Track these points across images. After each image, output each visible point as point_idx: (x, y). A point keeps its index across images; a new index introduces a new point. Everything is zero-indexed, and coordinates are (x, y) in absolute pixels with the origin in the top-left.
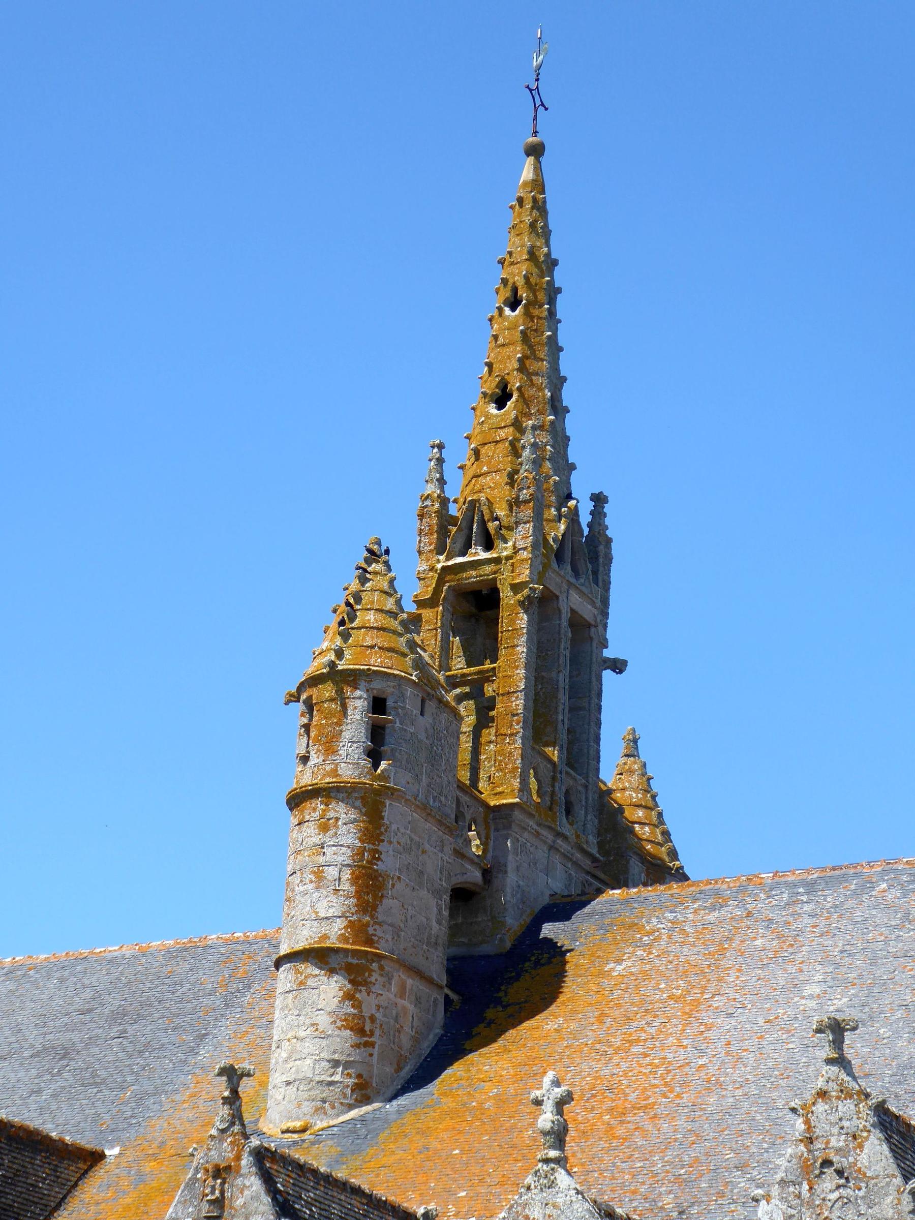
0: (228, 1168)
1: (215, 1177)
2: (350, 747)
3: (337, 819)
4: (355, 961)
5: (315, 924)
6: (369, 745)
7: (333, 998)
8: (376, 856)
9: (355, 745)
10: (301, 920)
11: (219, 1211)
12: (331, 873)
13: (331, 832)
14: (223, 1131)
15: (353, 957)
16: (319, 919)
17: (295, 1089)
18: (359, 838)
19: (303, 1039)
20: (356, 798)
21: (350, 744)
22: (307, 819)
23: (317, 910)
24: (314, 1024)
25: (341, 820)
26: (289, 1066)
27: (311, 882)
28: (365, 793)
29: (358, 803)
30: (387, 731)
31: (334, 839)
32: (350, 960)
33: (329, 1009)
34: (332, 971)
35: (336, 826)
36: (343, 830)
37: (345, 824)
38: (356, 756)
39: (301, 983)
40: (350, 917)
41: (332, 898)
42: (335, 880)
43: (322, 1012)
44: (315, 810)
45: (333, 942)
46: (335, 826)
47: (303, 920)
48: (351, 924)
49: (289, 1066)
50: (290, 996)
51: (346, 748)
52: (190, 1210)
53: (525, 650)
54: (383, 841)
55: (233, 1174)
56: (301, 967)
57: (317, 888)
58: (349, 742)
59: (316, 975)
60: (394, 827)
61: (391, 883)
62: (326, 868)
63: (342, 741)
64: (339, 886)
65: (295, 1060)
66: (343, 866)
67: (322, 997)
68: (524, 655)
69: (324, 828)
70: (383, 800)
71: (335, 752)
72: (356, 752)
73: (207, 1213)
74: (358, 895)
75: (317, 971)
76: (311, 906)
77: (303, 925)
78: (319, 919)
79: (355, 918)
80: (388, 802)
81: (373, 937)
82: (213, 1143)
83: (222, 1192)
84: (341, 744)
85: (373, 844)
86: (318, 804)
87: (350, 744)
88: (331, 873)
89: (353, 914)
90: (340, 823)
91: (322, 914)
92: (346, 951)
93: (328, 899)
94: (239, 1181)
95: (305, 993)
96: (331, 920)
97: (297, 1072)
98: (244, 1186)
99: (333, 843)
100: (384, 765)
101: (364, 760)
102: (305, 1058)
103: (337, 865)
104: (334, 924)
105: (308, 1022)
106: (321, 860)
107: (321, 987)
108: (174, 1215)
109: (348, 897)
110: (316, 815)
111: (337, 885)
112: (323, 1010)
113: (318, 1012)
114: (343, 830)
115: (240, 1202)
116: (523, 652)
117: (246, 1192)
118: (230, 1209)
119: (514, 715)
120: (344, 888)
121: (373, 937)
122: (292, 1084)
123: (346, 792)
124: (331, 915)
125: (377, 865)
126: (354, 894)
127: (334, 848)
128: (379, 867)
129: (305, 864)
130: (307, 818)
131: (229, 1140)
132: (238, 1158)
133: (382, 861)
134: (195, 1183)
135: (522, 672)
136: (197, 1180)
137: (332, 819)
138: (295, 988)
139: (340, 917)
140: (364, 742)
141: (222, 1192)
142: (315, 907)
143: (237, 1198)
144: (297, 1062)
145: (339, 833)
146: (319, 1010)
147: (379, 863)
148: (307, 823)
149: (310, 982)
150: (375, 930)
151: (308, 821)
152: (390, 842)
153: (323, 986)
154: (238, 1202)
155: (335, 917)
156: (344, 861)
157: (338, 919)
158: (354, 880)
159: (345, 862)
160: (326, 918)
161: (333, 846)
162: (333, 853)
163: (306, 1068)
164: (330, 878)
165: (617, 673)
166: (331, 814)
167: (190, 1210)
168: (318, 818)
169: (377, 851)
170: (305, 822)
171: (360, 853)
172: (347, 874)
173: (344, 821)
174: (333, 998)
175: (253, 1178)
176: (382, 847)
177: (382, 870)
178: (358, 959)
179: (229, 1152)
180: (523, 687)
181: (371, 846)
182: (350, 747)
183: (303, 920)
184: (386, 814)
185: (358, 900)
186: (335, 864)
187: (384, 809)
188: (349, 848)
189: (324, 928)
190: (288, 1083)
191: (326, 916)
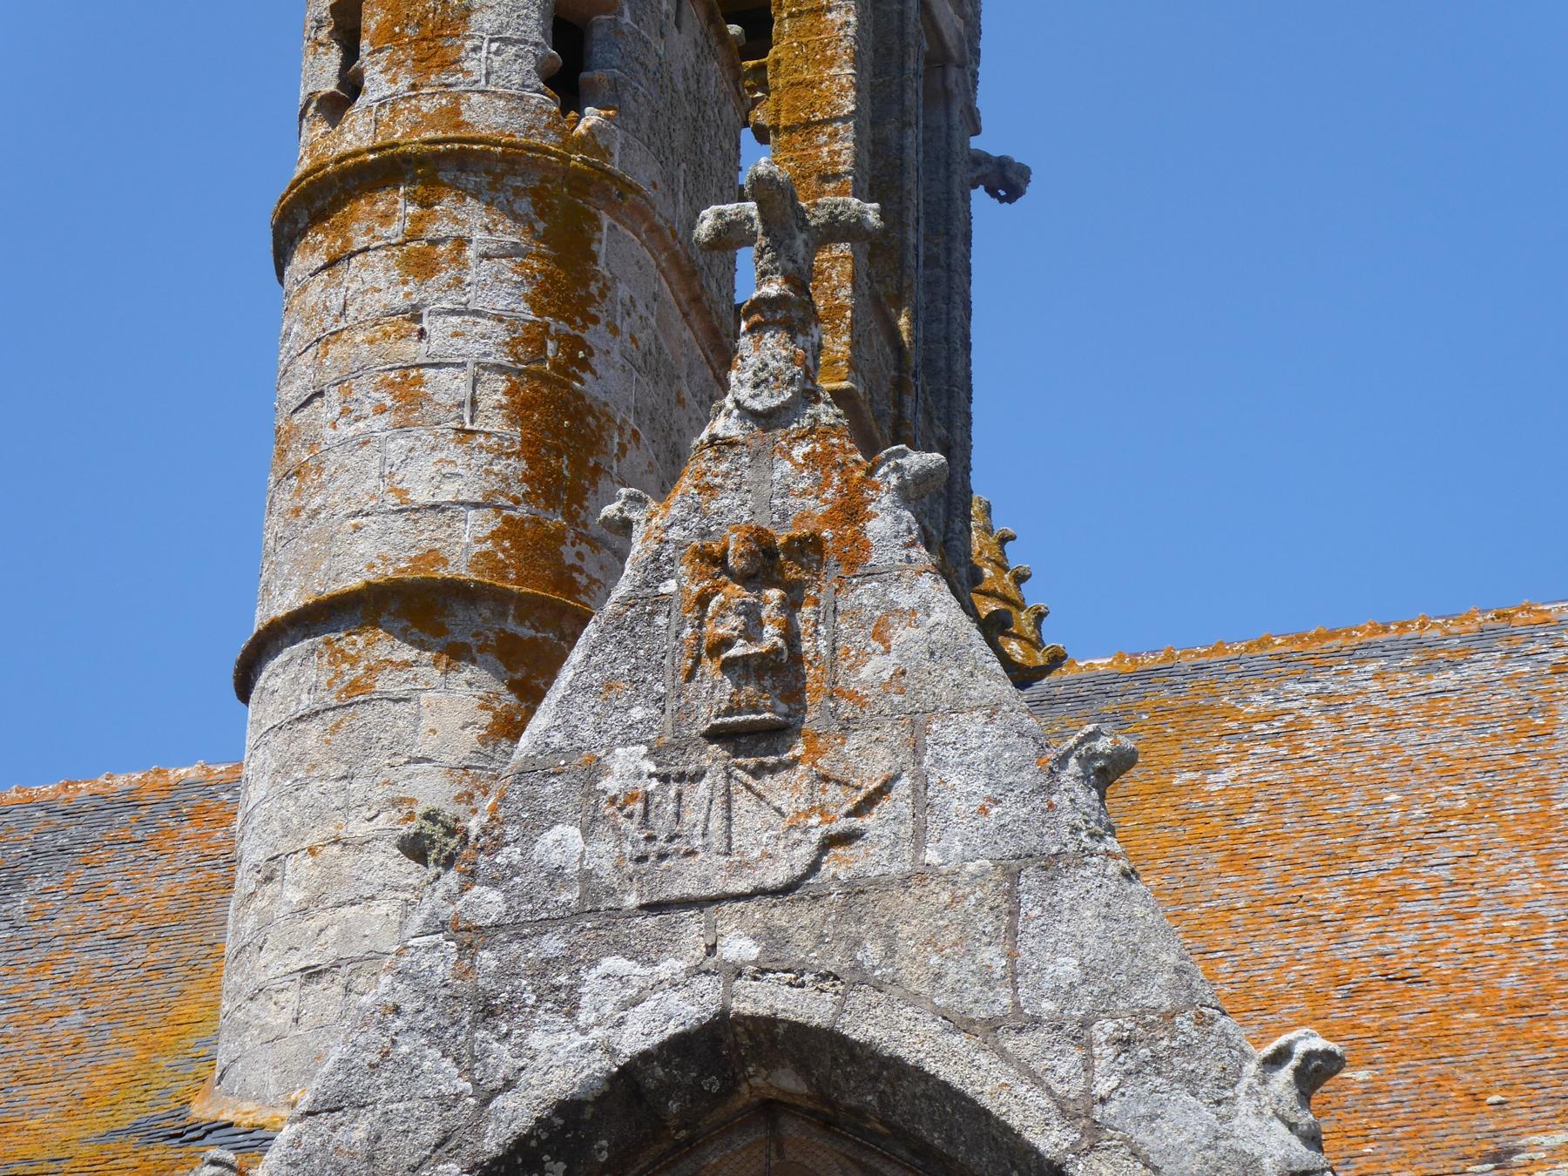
0: (808, 548)
1: (754, 578)
2: (497, 53)
3: (462, 243)
4: (526, 632)
5: (399, 522)
6: (552, 56)
7: (463, 728)
8: (577, 358)
9: (512, 50)
10: (348, 516)
11: (783, 708)
12: (448, 385)
13: (444, 277)
14: (766, 420)
15: (521, 619)
16: (408, 510)
17: (337, 989)
18: (528, 299)
19: (363, 844)
20: (517, 192)
21: (494, 46)
22: (361, 247)
23: (404, 485)
24: (403, 801)
25: (473, 245)
26: (314, 925)
27: (381, 410)
28: (542, 181)
29: (524, 205)
30: (598, 33)
31: (453, 295)
32: (511, 625)
33: (449, 759)
34: (457, 654)
35: (457, 258)
36: (478, 272)
37: (486, 256)
38: (516, 79)
39: (354, 686)
40: (507, 508)
41: (453, 452)
42: (461, 405)
43: (425, 765)
44: (386, 218)
45: (459, 568)
46: (454, 260)
47: (355, 515)
48: (511, 529)
49: (314, 925)
50: (314, 729)
51: (484, 53)
52: (637, 713)
53: (852, 19)
54: (595, 320)
55: (833, 570)
56: (354, 643)
57: (401, 427)
58: (491, 41)
59: (407, 664)
60: (623, 291)
61: (616, 440)
62: (431, 372)
63: (472, 37)
64: (472, 422)
65: (339, 905)
66: (485, 368)
67: (427, 722)
68: (851, 31)
69: (421, 265)
70: (592, 210)
71: (450, 64)
72: (516, 67)
73: (729, 712)
74: (531, 450)
75: (407, 653)
76: (382, 476)
77: (357, 528)
78: (408, 510)
79: (521, 512)
80: (606, 220)
81: (575, 575)
82: (724, 467)
83: (791, 635)
84: (469, 44)
85: (570, 322)
86: (401, 206)
87: (494, 46)
88: (448, 385)
89: (517, 502)
90: (470, 253)
91: (421, 496)
92: (501, 598)
93: (439, 455)
94: (865, 595)
95: (370, 714)
96: (450, 513)
97: (345, 937)
98: (893, 610)
99: (450, 306)
100: (592, 117)
101: (538, 91)
102: (373, 898)
103: (464, 364)
104: (462, 525)
105: (379, 794)
106: (413, 350)
107: (423, 695)
108: (557, 739)
109: (500, 454)
110: (395, 230)
111: (467, 420)
112: (429, 760)
113: (412, 767)
114: (478, 272)
115: (875, 668)
116: (847, 24)
117: (901, 634)
118: (831, 697)
119: (825, 178)
120: (487, 429)
121: (575, 575)
122: (328, 977)
123: (488, 172)
124: (449, 498)
125: (582, 381)
126: (518, 447)
127: (455, 320)
128: (587, 385)
129: (358, 364)
130: (360, 241)
131: (799, 452)
132: (852, 511)
133: (594, 373)
134: (652, 614)
135: (845, 72)
136: (660, 599)
137: (443, 240)
138: (334, 703)
139: (477, 506)
140: (536, 44)
141: (791, 635)
142: (399, 478)
143: (863, 656)
144: (345, 910)
145: (468, 279)
146: (418, 761)
147: (587, 376)
148: (360, 257)
149: (386, 683)
150: (580, 555)
151: (366, 249)
152: (615, 331)
153: (431, 694)
154: (866, 672)
155: (462, 503)
156: (485, 354)
157: (472, 512)
158: (519, 410)
159: (491, 360)
160: (434, 507)
161: (453, 312)
162: (450, 331)
163: (377, 927)
164: (441, 398)
165: (1002, 200)
166: (444, 228)
167: (637, 713)
168: (400, 239)
169: (580, 343)
170: (353, 254)
171: (534, 338)
172: (495, 392)
173: (483, 249)
174: (463, 728)
175: (926, 583)
176: (594, 336)
177: (596, 399)
178: (533, 626)
179: (804, 493)
180: (852, 108)
181: (563, 326)
182: (497, 53)
183: (355, 515)
184: (601, 249)
185: (532, 463)
186: (460, 360)
187: (597, 235)
188: (501, 321)
189: (428, 533)
190: (312, 974)
191: (433, 500)
